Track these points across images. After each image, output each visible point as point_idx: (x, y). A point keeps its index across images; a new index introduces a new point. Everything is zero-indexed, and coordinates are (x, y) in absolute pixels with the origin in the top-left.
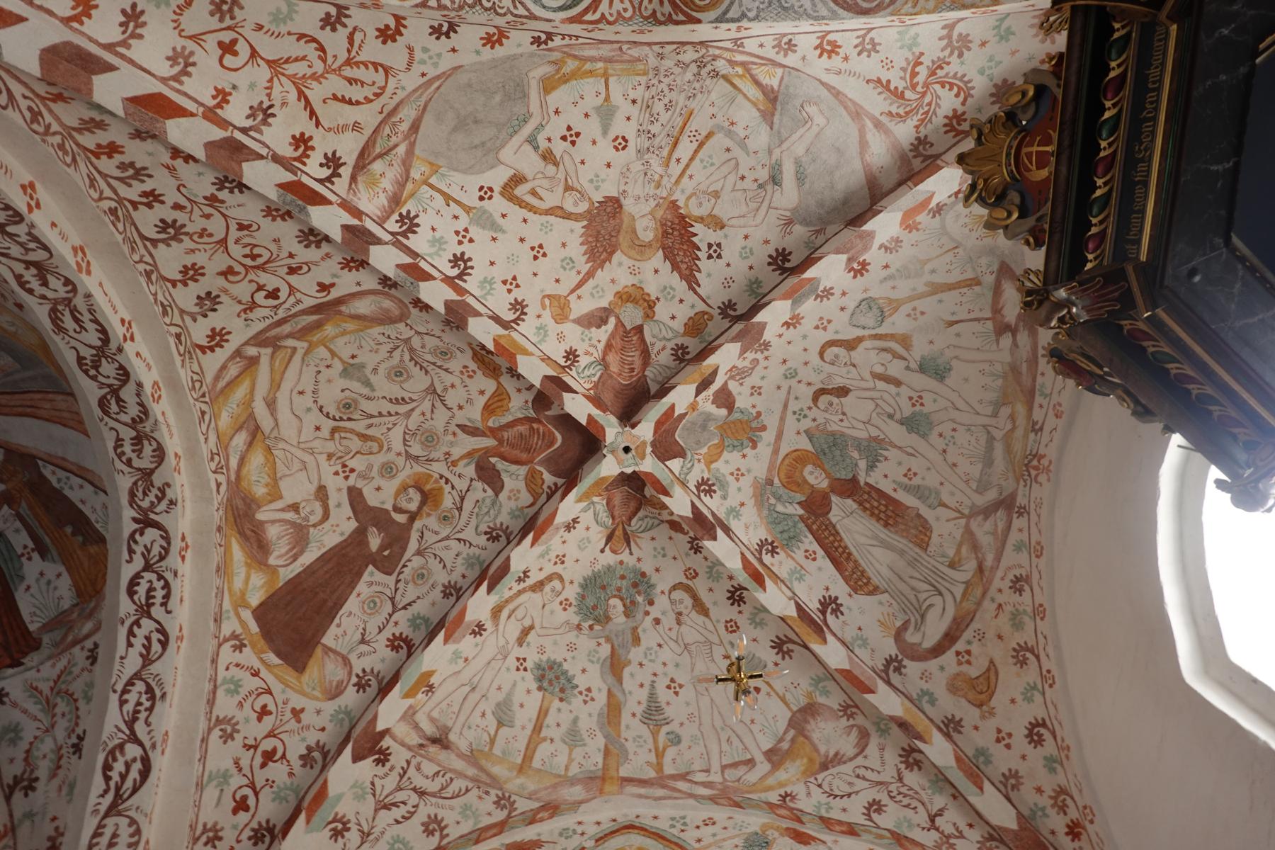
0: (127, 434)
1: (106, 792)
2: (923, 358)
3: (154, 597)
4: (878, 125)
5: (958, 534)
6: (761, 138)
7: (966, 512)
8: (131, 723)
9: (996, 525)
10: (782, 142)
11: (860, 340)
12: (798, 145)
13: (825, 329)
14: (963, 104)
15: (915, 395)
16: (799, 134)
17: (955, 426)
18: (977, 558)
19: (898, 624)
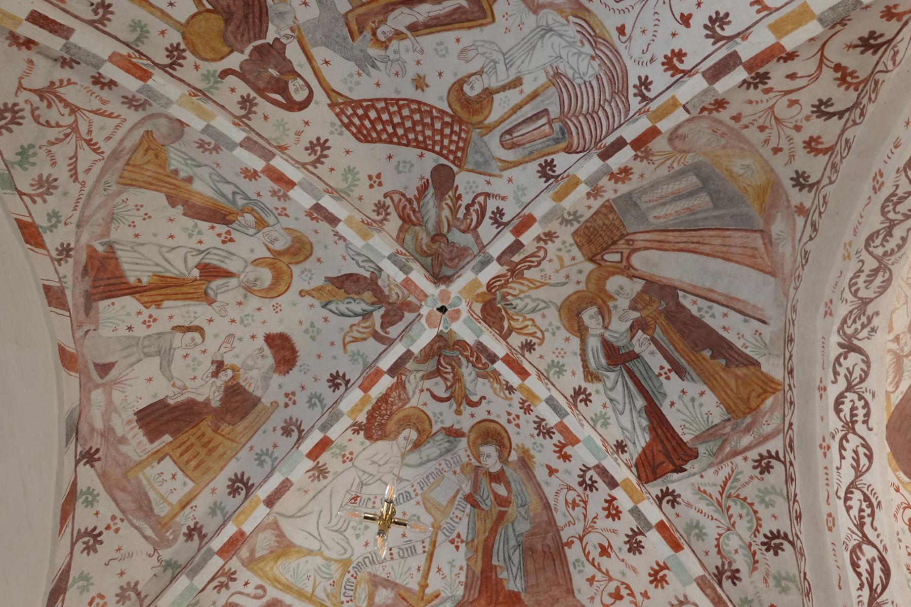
0: (871, 264)
1: (861, 587)
3: (856, 415)
8: (861, 526)
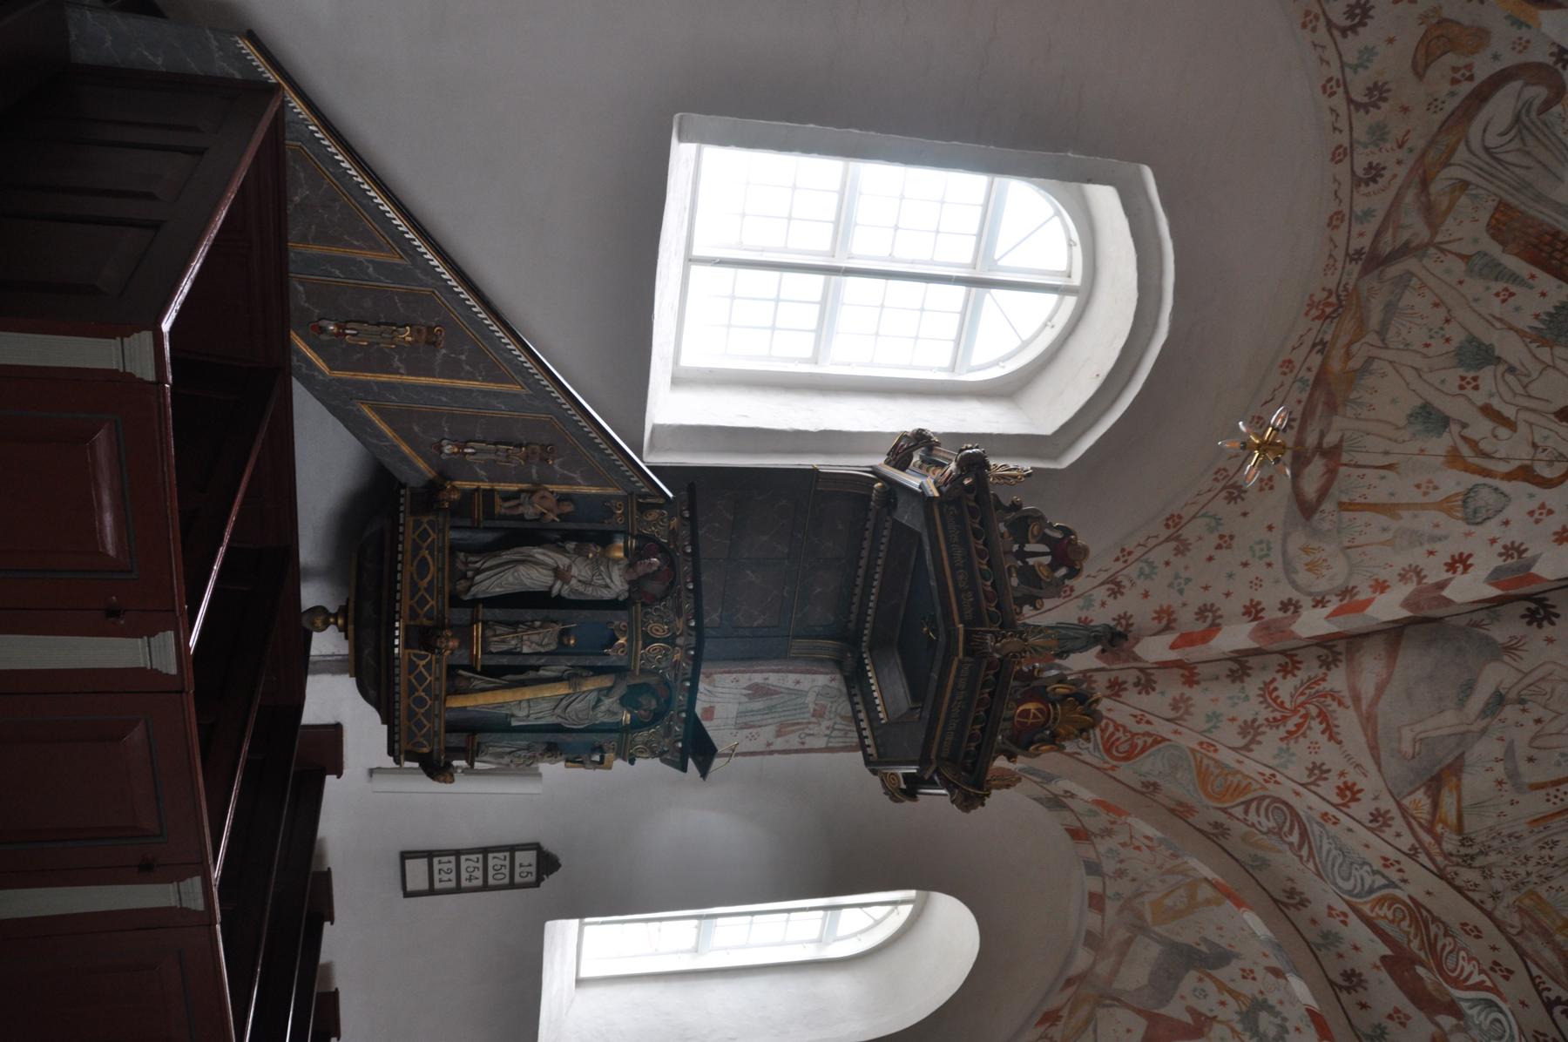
2: (1440, 435)
4: (1357, 699)
5: (1450, 222)
6: (1485, 751)
7: (1432, 251)
9: (1394, 236)
10: (1463, 734)
11: (1509, 476)
12: (1449, 721)
13: (1542, 506)
14: (1274, 680)
15: (1469, 391)
16: (1438, 733)
17: (1425, 350)
18: (1428, 195)
19: (1558, 109)
